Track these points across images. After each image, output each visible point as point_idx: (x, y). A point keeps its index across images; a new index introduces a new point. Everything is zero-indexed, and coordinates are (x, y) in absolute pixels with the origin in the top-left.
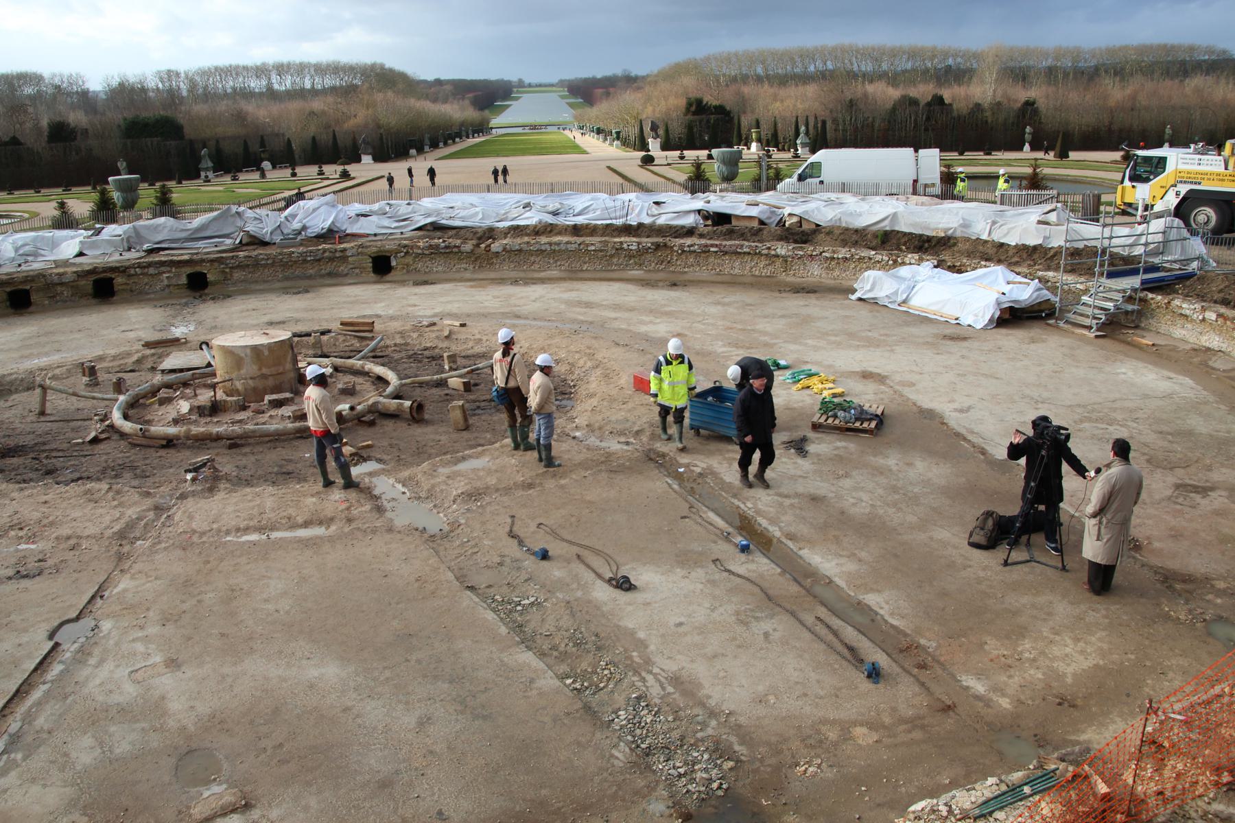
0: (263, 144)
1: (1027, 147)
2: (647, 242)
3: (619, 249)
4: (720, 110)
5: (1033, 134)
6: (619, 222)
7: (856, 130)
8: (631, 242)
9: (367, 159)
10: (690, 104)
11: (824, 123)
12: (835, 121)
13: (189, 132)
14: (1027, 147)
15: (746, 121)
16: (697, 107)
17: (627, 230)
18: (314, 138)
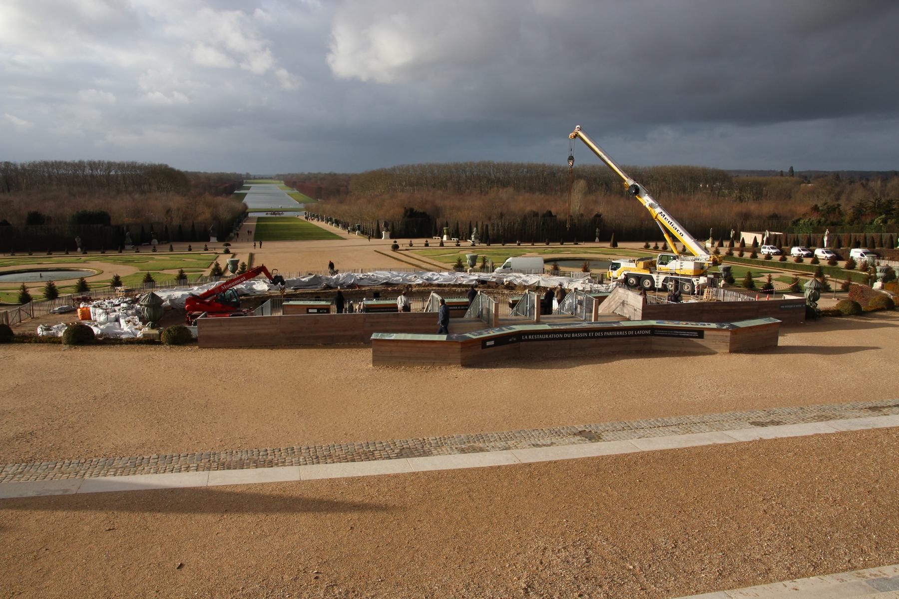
0: (152, 229)
1: (597, 239)
2: (464, 289)
3: (455, 292)
4: (423, 215)
5: (600, 232)
6: (452, 283)
7: (504, 230)
8: (459, 290)
9: (213, 239)
10: (406, 211)
11: (487, 226)
12: (493, 225)
13: (113, 222)
14: (597, 239)
15: (439, 222)
16: (411, 214)
17: (455, 286)
18: (180, 227)
